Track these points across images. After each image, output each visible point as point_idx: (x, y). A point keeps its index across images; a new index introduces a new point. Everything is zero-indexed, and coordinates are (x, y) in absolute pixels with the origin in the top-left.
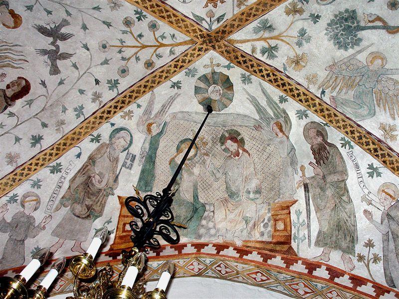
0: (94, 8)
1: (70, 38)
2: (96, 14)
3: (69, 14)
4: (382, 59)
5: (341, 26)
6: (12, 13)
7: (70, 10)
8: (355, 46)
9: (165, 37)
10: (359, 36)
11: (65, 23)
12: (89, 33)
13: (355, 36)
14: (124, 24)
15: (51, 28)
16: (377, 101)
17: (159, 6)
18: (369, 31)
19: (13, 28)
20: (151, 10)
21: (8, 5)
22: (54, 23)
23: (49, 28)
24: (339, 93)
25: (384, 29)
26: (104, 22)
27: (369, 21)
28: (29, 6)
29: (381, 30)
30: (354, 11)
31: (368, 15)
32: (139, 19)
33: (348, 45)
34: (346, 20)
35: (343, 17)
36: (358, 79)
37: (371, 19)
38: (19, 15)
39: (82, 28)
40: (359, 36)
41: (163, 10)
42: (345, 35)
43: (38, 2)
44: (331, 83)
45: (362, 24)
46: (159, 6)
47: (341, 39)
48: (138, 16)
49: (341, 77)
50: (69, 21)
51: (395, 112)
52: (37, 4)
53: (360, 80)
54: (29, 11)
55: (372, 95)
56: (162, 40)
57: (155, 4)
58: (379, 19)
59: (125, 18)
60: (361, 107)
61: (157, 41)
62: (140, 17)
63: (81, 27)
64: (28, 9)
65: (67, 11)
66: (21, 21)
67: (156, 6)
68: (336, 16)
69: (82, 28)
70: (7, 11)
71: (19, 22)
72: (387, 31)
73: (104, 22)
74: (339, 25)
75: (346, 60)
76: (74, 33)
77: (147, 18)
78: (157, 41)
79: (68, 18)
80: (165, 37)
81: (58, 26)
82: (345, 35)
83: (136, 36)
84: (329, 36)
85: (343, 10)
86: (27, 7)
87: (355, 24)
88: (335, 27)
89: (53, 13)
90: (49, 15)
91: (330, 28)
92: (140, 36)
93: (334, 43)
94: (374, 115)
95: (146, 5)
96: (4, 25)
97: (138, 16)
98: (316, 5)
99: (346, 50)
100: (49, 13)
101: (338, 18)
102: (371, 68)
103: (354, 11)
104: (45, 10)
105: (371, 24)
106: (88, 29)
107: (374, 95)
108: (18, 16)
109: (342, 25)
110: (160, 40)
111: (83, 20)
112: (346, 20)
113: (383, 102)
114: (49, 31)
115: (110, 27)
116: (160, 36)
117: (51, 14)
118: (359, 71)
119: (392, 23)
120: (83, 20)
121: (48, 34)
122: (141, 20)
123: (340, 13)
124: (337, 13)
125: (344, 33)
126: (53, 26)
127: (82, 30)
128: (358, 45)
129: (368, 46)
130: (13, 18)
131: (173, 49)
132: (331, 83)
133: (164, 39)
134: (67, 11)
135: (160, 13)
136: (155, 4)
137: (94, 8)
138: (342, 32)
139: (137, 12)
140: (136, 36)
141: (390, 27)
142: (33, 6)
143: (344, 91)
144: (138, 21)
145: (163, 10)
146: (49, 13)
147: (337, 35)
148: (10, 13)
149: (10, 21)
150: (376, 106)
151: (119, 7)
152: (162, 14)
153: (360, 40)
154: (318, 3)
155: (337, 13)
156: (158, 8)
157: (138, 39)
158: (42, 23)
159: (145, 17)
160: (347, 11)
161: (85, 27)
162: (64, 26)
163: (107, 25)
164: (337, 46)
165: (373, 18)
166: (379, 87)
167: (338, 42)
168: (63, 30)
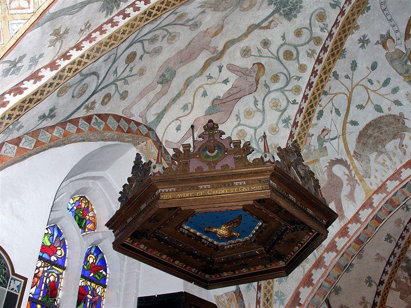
10: (273, 5)
13: (275, 4)
18: (267, 15)
25: (259, 24)
29: (259, 22)
30: (290, 20)
31: (278, 24)
34: (291, 10)
35: (295, 10)
37: (273, 23)
40: (273, 5)
45: (277, 15)
58: (268, 27)
68: (301, 7)
72: (255, 25)
74: (294, 2)
85: (299, 15)
87: (281, 11)
98: (322, 6)
101: (298, 7)
103: (290, 20)
105: (270, 19)
109: (291, 4)
112: (291, 10)
119: (257, 31)
123: (299, 12)
124: (301, 10)
129: (261, 5)
153: (270, 4)
154: (322, 9)
155: (301, 10)
160: (295, 16)
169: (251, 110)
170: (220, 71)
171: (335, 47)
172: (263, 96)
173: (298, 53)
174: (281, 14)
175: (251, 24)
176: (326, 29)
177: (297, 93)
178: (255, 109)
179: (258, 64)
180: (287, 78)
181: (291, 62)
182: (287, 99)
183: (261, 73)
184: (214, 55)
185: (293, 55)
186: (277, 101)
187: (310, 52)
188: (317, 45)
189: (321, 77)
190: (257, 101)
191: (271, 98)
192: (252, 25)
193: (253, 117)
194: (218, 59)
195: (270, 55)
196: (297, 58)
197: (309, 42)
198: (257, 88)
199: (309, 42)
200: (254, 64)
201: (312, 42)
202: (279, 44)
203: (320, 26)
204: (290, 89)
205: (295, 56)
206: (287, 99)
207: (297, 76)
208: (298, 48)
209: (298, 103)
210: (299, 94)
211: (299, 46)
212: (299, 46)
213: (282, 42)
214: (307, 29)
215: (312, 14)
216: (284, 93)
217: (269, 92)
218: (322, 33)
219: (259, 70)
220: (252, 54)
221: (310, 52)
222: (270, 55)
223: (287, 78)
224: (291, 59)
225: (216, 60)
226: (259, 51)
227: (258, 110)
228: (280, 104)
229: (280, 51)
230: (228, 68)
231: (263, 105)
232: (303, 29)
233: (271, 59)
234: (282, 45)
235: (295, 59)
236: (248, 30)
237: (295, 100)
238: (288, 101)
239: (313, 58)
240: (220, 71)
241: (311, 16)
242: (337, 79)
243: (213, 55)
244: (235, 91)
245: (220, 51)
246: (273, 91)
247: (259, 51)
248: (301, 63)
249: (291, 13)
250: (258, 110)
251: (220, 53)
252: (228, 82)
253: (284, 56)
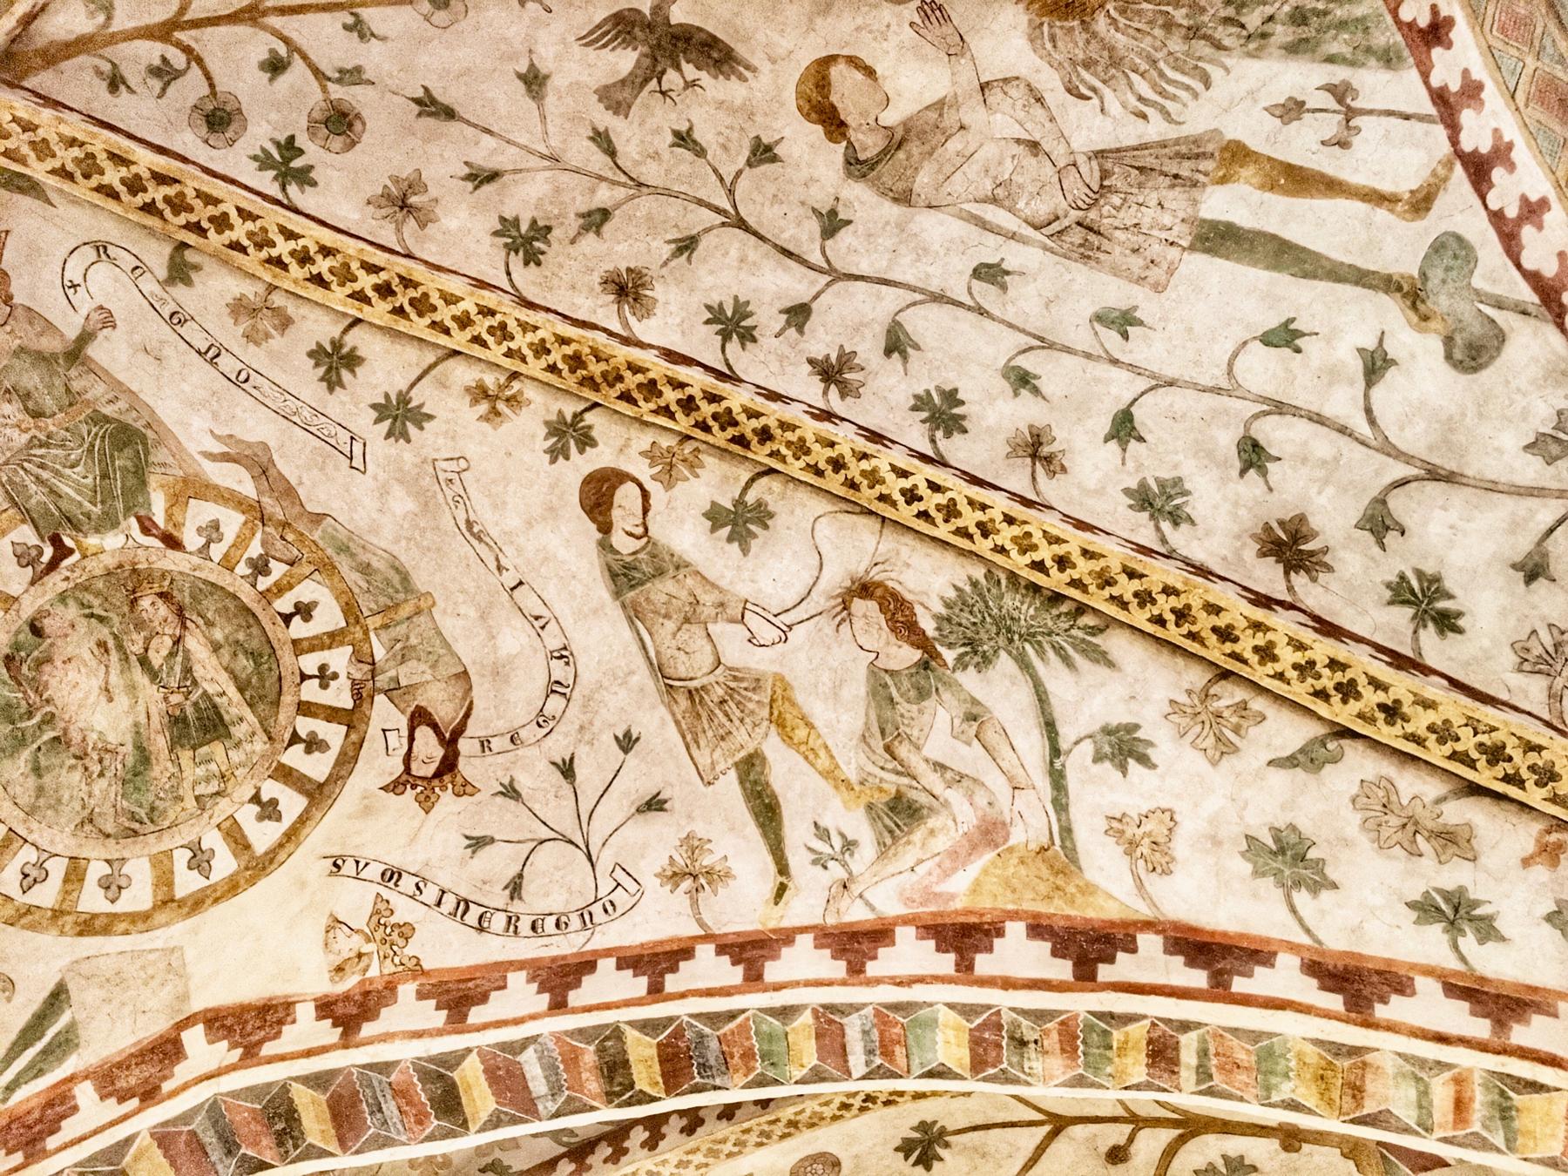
0: (493, 176)
1: (599, 27)
2: (486, 153)
3: (603, 140)
6: (832, 122)
7: (598, 161)
9: (155, 72)
11: (616, 98)
12: (512, 57)
14: (358, 116)
15: (678, 68)
17: (188, 226)
19: (831, 60)
20: (222, 208)
21: (848, 163)
22: (663, 93)
23: (689, 70)
26: (449, 114)
28: (761, 162)
32: (290, 147)
38: (807, 116)
39: (546, 77)
41: (168, 213)
43: (728, 180)
46: (188, 226)
48: (297, 163)
50: (601, 106)
52: (733, 169)
54: (765, 140)
56: (164, 59)
57: (212, 233)
59: (353, 144)
61: (187, 50)
62: (287, 161)
63: (549, 83)
64: (768, 149)
65: (611, 152)
66: (800, 94)
67: (205, 224)
69: (546, 77)
70: (852, 134)
71: (809, 88)
73: (449, 114)
76: (576, 49)
77: (255, 158)
78: (187, 50)
79: (605, 119)
80: (155, 72)
81: (646, 81)
83: (298, 64)
86: (775, 159)
89: (670, 139)
90: (683, 128)
92: (275, 66)
95: (250, 225)
96: (870, 72)
97: (297, 163)
100: (684, 139)
104: (700, 152)
106: (520, 76)
108: (813, 115)
110: (178, 59)
111: (543, 118)
114: (684, 52)
115: (420, 93)
116: (178, 74)
117: (677, 134)
120: (543, 118)
121: (688, 40)
122: (278, 144)
126: (672, 78)
127: (544, 71)
130: (833, 107)
131: (101, 18)
133: (157, 62)
134: (611, 152)
135: (181, 195)
136: (212, 233)
137: (493, 176)
139: (304, 177)
140: (298, 64)
142: (749, 164)
144: (292, 139)
145: (168, 213)
146: (684, 139)
148: (842, 124)
149: (846, 88)
151: (386, 195)
152: (170, 191)
156: (193, 218)
157: (282, 50)
158: (714, 87)
159: (264, 162)
161: (534, 81)
162: (623, 82)
163: (434, 101)
168: (625, 60)
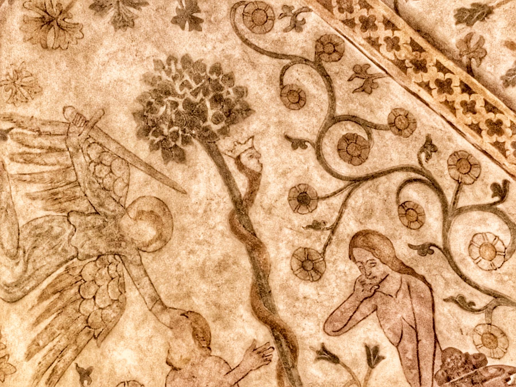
4: (160, 237)
5: (195, 93)
8: (159, 152)
10: (188, 149)
13: (186, 141)
16: (50, 285)
18: (214, 170)
24: (21, 178)
25: (235, 202)
27: (239, 157)
29: (227, 198)
30: (248, 110)
31: (252, 147)
33: (155, 134)
35: (221, 88)
36: (83, 205)
37: (244, 159)
40: (188, 149)
42: (178, 113)
44: (36, 142)
47: (162, 110)
49: (64, 159)
51: (47, 348)
53: (81, 213)
55: (59, 266)
60: (14, 257)
68: (217, 69)
74: (194, 86)
75: (113, 147)
82: (178, 113)
84: (157, 74)
85: (240, 81)
87: (215, 128)
88: (187, 77)
91: (180, 66)
93: (144, 95)
94: (14, 301)
99: (139, 135)
101: (214, 77)
102: (125, 222)
103: (248, 110)
107: (62, 270)
109: (201, 96)
112: (217, 100)
113: (54, 303)
118: (103, 194)
123: (230, 78)
124: (226, 70)
125: (180, 108)
128: (166, 158)
132: (36, 142)
138: (180, 101)
141: (246, 215)
143: (34, 189)
147: (167, 93)
150: (37, 292)
153: (182, 158)
154: (234, 9)
155: (226, 70)
160: (242, 92)
164: (139, 107)
165: (252, 164)
166: (89, 270)
167: (150, 104)
169: (482, 330)
170: (334, 359)
171: (341, 10)
172: (450, 275)
173: (353, 119)
174: (224, 132)
175: (226, 223)
176: (296, 15)
177: (475, 172)
178: (480, 318)
179: (353, 245)
180: (416, 180)
181: (374, 149)
182: (482, 208)
183: (386, 251)
184: (275, 355)
185: (356, 137)
186: (479, 241)
187: (358, 82)
188: (341, 55)
189: (427, 86)
190: (462, 298)
191: (466, 253)
192: (231, 220)
193: (503, 334)
194: (294, 350)
195: (337, 201)
196: (368, 126)
197: (326, 76)
198: (423, 279)
199: (326, 76)
200: (351, 257)
201: (332, 68)
202: (313, 162)
203: (285, 30)
204: (455, 185)
205: (362, 133)
206: (482, 208)
207: (421, 151)
208: (340, 112)
209: (505, 182)
210: (478, 165)
211: (332, 107)
212: (332, 107)
213: (310, 152)
214: (286, 68)
215: (246, 41)
216: (460, 211)
217: (446, 251)
218: (307, 28)
219: (372, 249)
220: (319, 248)
221: (358, 82)
222: (337, 201)
223: (416, 180)
224: (367, 147)
225: (295, 358)
226: (316, 226)
227: (488, 310)
228: (491, 239)
229: (335, 167)
230: (337, 332)
231: (477, 287)
232: (285, 82)
233: (351, 202)
234: (319, 156)
235: (369, 134)
236: (242, 238)
237: (495, 186)
238: (491, 208)
239: (379, 81)
240: (334, 359)
241: (250, 45)
242: (490, 12)
243: (273, 366)
244: (409, 345)
245: (272, 340)
246: (445, 237)
247: (316, 226)
248: (385, 122)
249: (227, 101)
250: (488, 310)
251: (277, 338)
252: (376, 349)
253: (350, 161)
